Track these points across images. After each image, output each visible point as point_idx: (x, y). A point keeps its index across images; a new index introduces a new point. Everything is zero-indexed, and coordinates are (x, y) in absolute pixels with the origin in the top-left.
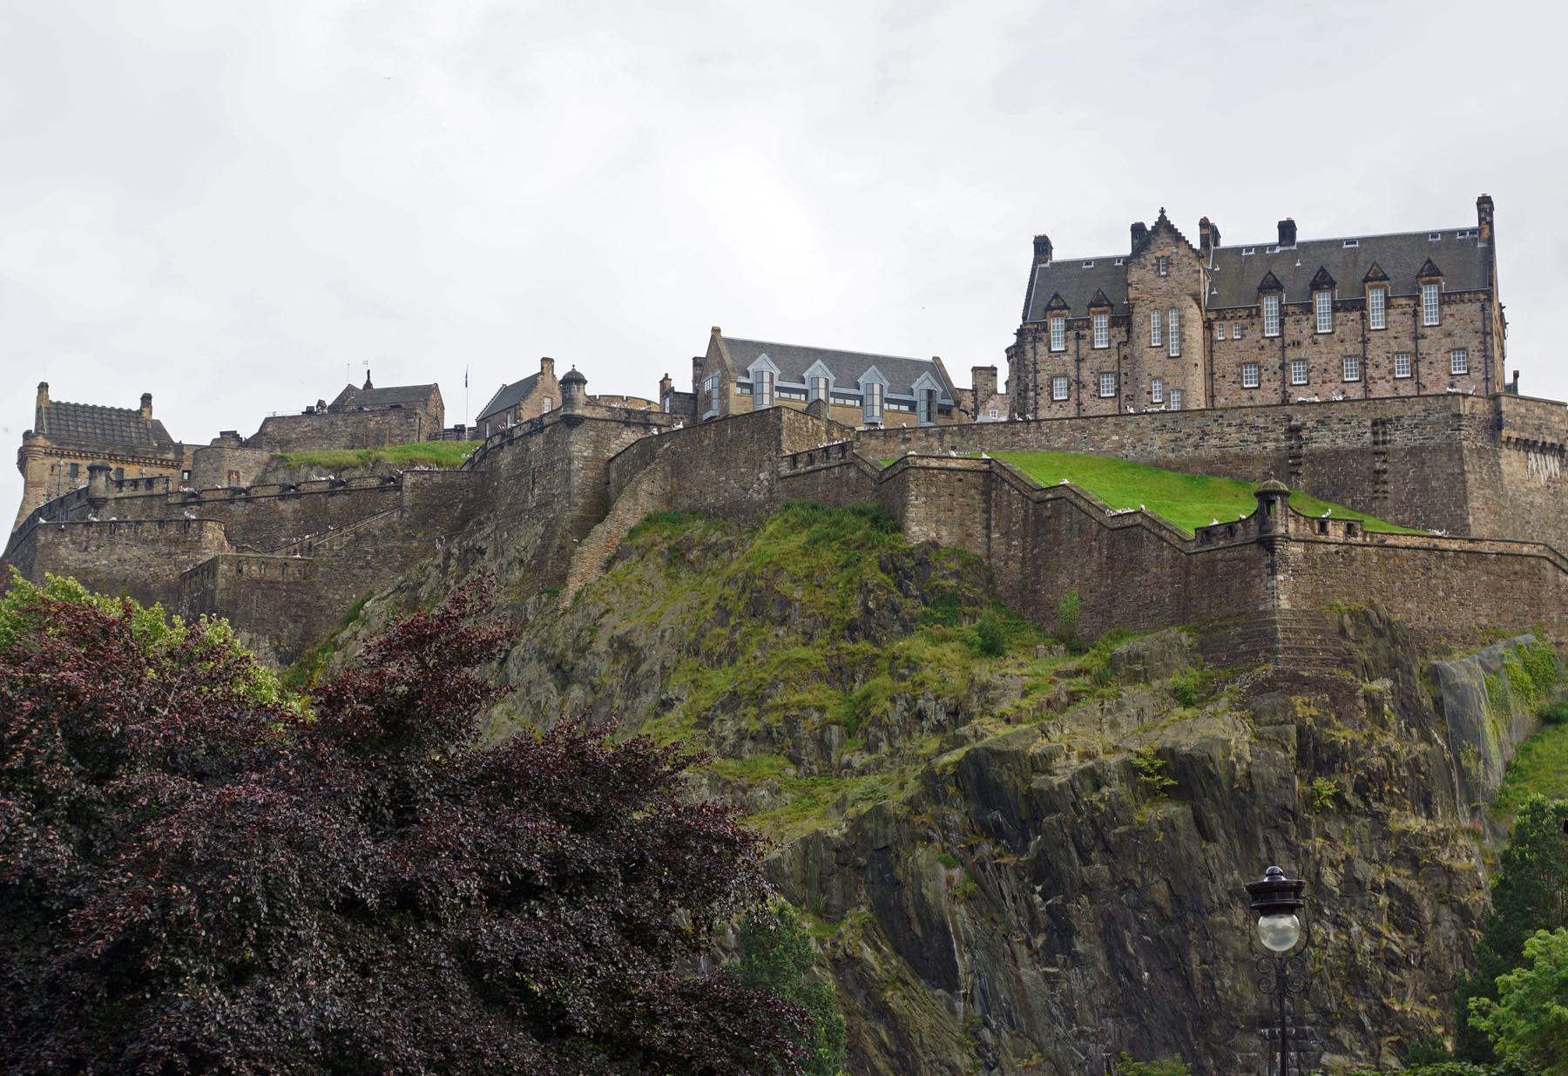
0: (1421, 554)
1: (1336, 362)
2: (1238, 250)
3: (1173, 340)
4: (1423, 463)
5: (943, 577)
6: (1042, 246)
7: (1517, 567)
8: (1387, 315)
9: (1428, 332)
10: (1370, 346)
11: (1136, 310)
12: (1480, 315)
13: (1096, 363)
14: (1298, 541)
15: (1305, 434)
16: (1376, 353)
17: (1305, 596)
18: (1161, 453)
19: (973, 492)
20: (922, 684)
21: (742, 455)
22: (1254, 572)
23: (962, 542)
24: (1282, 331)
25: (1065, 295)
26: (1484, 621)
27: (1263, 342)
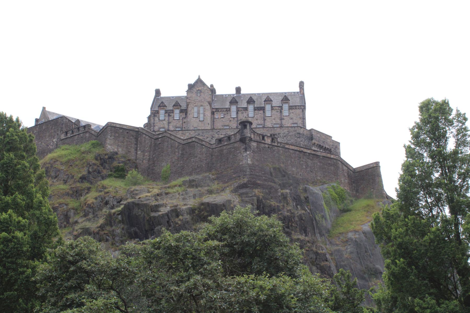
0: (297, 153)
2: (222, 95)
3: (202, 116)
5: (119, 163)
6: (158, 92)
7: (329, 162)
8: (272, 112)
9: (285, 118)
10: (266, 121)
11: (189, 106)
12: (302, 113)
13: (175, 124)
14: (255, 141)
17: (257, 160)
19: (132, 137)
20: (108, 192)
21: (48, 134)
22: (238, 152)
23: (127, 153)
24: (237, 116)
26: (319, 178)
27: (231, 119)
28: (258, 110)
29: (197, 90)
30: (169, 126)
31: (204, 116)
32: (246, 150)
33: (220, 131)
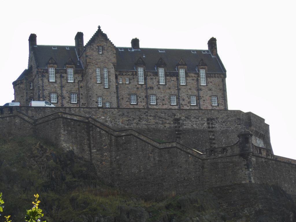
1: (167, 97)
3: (106, 81)
4: (228, 137)
6: (33, 38)
9: (203, 88)
10: (181, 92)
15: (181, 122)
16: (183, 95)
18: (123, 125)
27: (138, 86)
28: (171, 76)
30: (62, 90)
31: (109, 81)
32: (248, 166)
33: (149, 112)
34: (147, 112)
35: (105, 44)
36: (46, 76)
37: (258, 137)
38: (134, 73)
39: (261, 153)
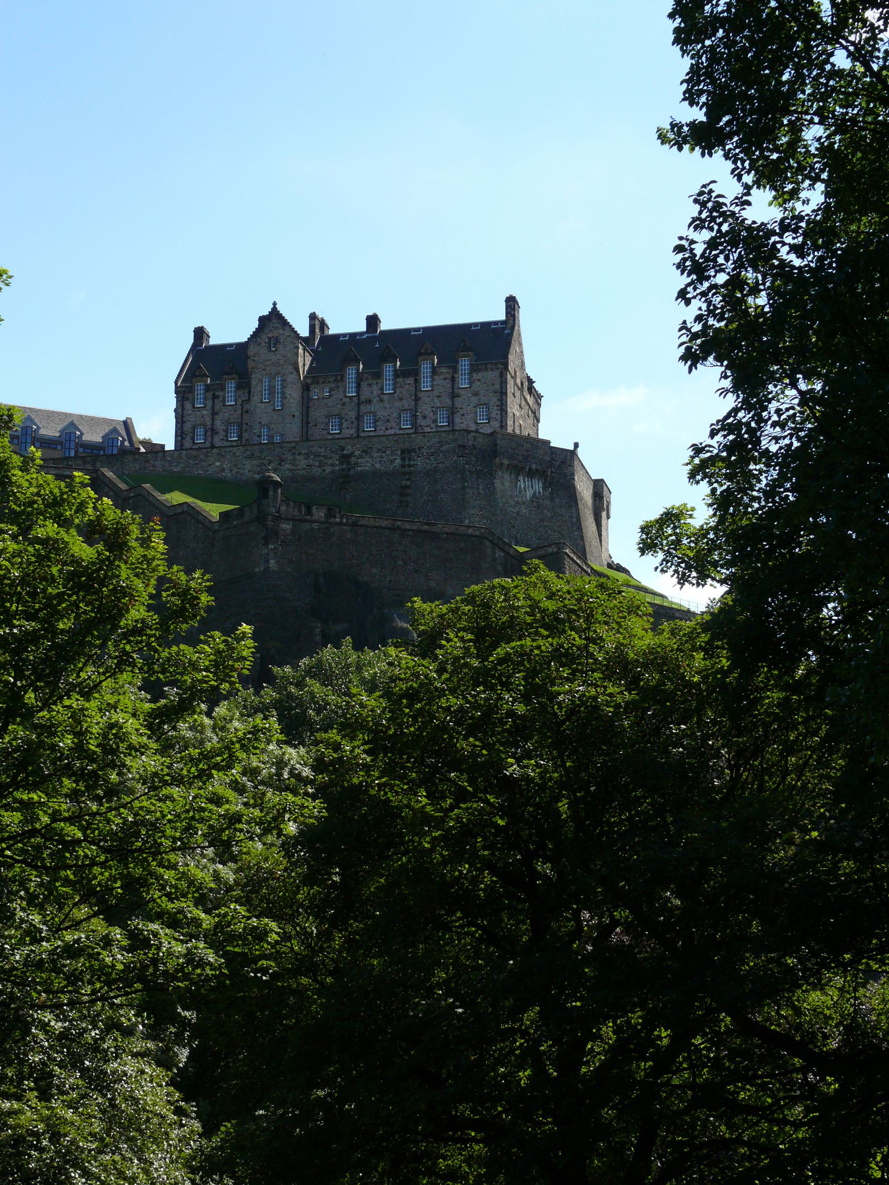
1: (395, 415)
2: (337, 336)
3: (278, 398)
6: (200, 333)
7: (462, 545)
8: (433, 380)
9: (462, 392)
10: (420, 403)
11: (253, 376)
12: (499, 380)
14: (288, 519)
15: (353, 460)
16: (425, 408)
24: (358, 392)
25: (209, 369)
26: (433, 584)
29: (270, 339)
30: (213, 420)
31: (284, 397)
32: (266, 541)
34: (294, 448)
35: (282, 332)
36: (191, 398)
37: (524, 477)
38: (339, 378)
39: (309, 512)
